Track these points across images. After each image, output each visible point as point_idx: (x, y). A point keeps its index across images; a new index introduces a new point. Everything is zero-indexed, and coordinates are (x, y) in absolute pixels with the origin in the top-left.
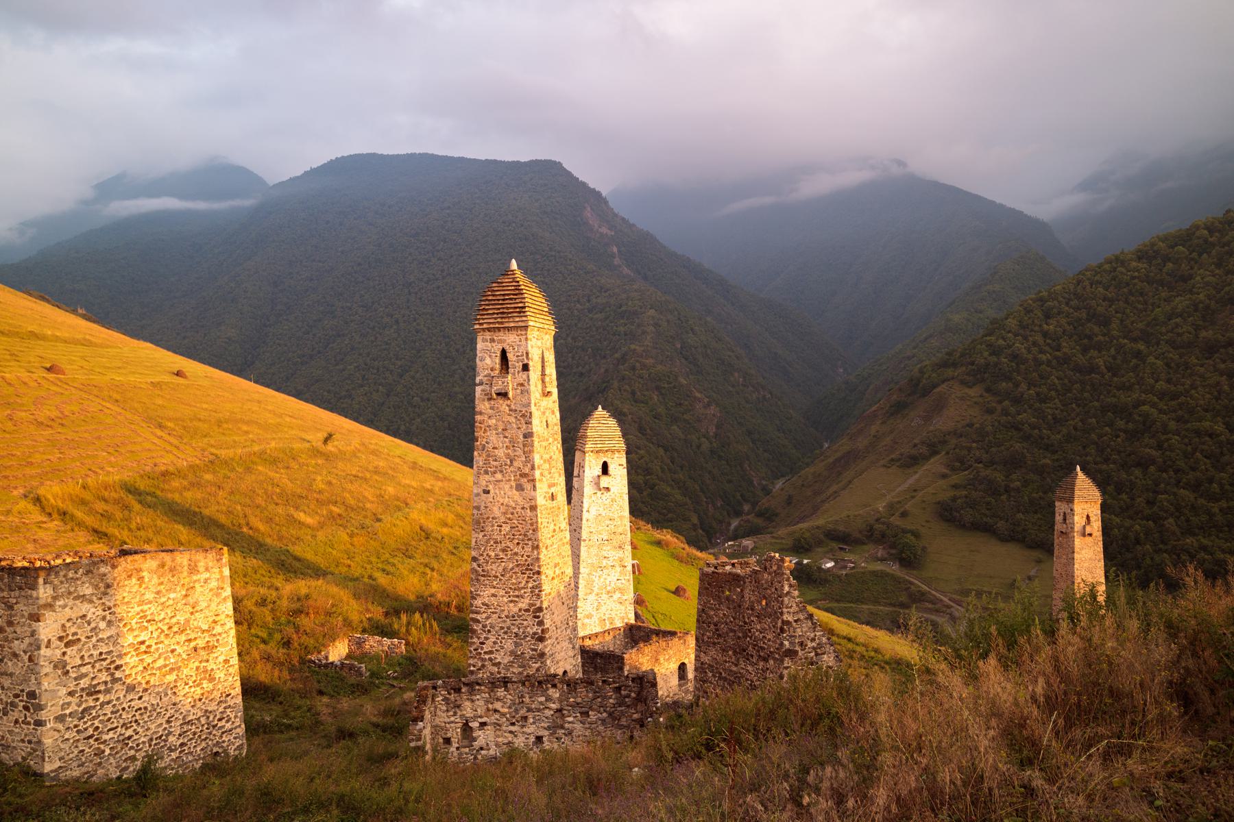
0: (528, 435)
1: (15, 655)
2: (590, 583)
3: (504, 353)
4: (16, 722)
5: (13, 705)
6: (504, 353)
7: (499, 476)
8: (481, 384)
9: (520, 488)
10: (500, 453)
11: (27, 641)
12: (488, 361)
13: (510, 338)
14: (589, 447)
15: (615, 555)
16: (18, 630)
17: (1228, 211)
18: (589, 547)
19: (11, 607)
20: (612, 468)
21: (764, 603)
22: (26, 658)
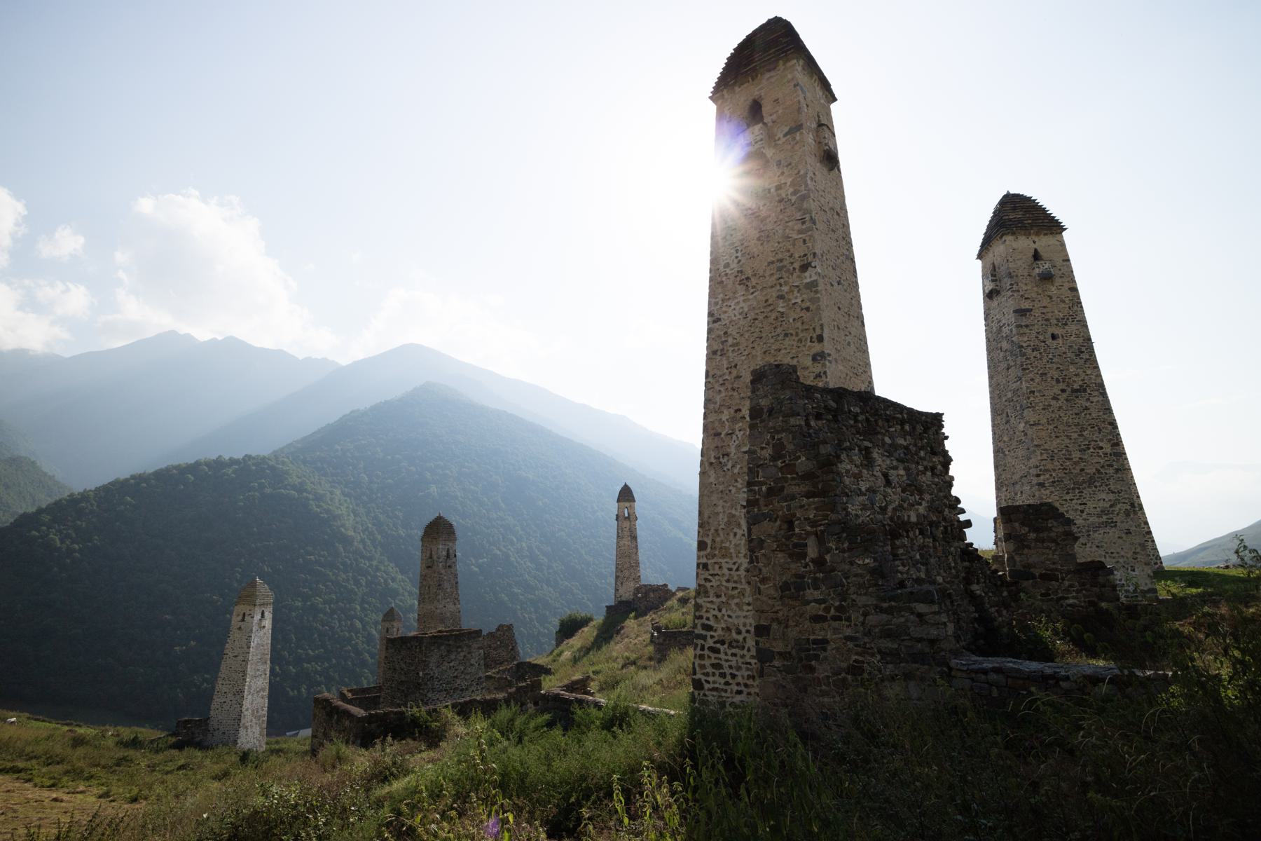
0: (457, 583)
1: (472, 665)
2: (250, 687)
3: (448, 550)
4: (473, 691)
5: (471, 685)
6: (448, 550)
7: (448, 600)
8: (441, 562)
9: (455, 604)
10: (449, 590)
11: (477, 658)
12: (444, 553)
13: (451, 544)
14: (258, 602)
15: (261, 667)
16: (473, 655)
17: (220, 456)
18: (252, 664)
19: (470, 646)
20: (266, 614)
21: (499, 643)
22: (477, 665)
